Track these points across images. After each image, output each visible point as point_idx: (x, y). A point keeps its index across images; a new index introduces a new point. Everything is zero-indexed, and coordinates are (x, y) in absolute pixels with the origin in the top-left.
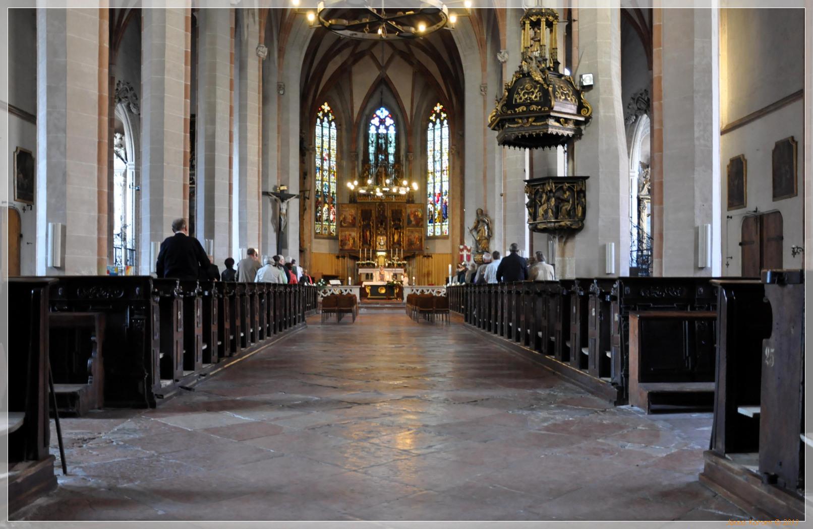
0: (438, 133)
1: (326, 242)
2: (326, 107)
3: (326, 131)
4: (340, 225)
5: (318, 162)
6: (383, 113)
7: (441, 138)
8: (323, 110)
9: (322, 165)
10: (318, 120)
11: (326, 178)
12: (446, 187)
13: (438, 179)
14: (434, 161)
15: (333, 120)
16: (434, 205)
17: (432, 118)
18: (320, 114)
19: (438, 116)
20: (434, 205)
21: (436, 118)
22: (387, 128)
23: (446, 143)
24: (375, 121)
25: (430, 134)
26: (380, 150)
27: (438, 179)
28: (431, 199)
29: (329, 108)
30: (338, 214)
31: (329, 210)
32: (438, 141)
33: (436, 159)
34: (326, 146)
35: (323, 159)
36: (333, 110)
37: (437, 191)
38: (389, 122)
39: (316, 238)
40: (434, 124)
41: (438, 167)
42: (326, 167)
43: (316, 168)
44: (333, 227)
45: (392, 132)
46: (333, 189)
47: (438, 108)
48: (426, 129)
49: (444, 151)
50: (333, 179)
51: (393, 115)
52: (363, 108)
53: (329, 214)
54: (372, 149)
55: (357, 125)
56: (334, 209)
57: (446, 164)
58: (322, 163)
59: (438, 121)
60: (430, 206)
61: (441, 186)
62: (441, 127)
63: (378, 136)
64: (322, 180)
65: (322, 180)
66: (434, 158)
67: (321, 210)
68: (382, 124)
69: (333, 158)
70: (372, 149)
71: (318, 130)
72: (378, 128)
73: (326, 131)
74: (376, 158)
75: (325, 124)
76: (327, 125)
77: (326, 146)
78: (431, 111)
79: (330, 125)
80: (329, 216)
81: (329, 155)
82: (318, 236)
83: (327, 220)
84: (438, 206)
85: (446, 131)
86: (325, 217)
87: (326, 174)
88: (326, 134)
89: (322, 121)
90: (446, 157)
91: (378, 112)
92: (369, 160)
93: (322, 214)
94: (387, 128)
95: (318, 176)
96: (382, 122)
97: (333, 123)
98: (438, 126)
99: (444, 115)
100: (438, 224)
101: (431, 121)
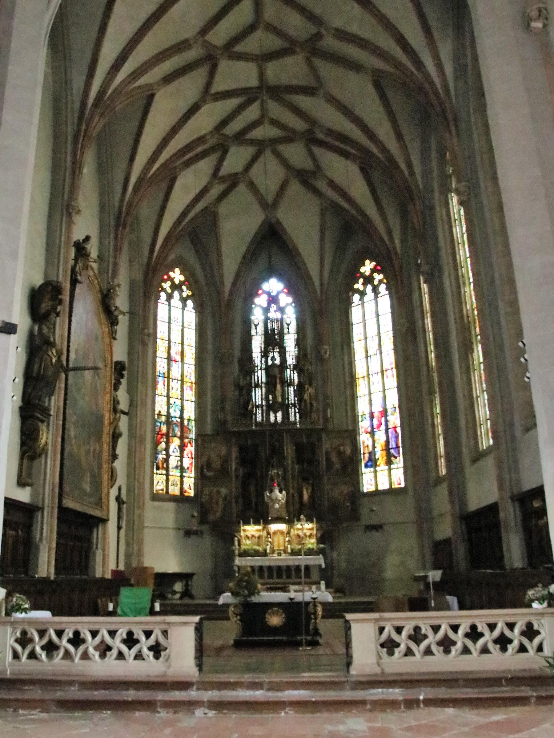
1: (171, 506)
3: (176, 313)
4: (201, 478)
5: (161, 365)
6: (273, 285)
8: (172, 280)
10: (163, 295)
11: (175, 392)
12: (393, 399)
13: (376, 387)
15: (188, 297)
16: (372, 433)
18: (167, 285)
19: (369, 280)
20: (372, 433)
22: (282, 310)
24: (261, 301)
26: (273, 340)
27: (376, 387)
28: (364, 425)
29: (182, 278)
31: (182, 447)
34: (176, 338)
35: (169, 358)
36: (191, 280)
37: (377, 408)
38: (285, 300)
41: (375, 366)
42: (176, 372)
44: (189, 482)
45: (291, 316)
46: (190, 412)
48: (348, 303)
50: (190, 395)
51: (291, 289)
52: (238, 276)
53: (182, 457)
54: (257, 344)
55: (229, 305)
56: (190, 449)
59: (369, 288)
60: (364, 439)
62: (376, 297)
63: (266, 321)
67: (167, 449)
68: (274, 304)
70: (257, 344)
71: (162, 310)
72: (266, 310)
73: (176, 313)
74: (265, 354)
75: (176, 301)
76: (180, 304)
77: (176, 338)
79: (184, 305)
80: (181, 460)
82: (156, 497)
83: (177, 467)
84: (380, 436)
85: (385, 301)
86: (173, 461)
87: (175, 385)
88: (176, 321)
89: (170, 297)
93: (168, 455)
94: (282, 310)
95: (161, 389)
96: (273, 300)
97: (190, 303)
99: (378, 277)
100: (382, 467)
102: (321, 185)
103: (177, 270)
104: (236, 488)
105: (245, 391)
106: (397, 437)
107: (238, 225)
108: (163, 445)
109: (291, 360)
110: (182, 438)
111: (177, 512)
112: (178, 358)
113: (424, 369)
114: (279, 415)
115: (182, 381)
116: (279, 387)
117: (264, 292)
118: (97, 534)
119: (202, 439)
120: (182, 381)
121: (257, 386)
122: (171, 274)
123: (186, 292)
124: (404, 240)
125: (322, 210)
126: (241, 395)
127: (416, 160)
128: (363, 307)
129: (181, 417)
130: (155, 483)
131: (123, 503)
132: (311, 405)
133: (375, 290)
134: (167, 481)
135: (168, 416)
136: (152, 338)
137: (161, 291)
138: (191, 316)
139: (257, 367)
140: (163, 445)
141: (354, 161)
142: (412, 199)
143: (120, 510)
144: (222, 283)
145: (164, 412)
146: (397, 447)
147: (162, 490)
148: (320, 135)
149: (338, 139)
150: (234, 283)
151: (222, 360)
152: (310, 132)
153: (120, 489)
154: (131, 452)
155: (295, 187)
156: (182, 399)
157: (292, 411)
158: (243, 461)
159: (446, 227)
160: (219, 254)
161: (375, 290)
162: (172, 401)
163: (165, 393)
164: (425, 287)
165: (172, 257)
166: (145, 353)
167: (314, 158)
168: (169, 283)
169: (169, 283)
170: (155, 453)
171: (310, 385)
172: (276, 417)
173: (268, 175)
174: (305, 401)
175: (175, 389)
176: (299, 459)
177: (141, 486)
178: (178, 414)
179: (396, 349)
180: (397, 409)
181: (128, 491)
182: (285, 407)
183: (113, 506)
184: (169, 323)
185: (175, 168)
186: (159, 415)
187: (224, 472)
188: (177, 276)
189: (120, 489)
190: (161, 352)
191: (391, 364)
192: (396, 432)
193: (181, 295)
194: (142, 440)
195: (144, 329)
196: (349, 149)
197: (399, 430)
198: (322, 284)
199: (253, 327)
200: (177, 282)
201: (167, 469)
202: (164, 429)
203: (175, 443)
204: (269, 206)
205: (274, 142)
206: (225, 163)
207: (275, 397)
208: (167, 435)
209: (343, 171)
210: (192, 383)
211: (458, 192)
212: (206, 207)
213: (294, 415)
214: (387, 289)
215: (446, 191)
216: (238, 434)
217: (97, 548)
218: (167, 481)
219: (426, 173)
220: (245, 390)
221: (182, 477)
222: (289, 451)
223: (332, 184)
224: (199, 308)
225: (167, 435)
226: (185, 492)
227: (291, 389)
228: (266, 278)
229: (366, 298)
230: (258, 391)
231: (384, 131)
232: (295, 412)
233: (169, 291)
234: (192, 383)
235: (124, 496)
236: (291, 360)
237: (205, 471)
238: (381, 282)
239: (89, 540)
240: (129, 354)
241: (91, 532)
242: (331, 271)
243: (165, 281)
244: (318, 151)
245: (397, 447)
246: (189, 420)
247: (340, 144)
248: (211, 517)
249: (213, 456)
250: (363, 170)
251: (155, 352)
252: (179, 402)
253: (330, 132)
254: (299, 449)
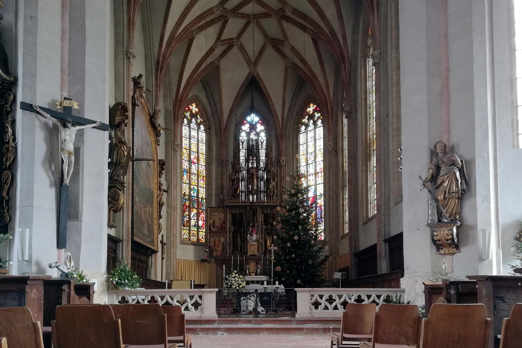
0: (311, 134)
1: (192, 247)
3: (194, 133)
4: (209, 232)
5: (185, 165)
7: (315, 140)
8: (191, 111)
9: (190, 168)
10: (185, 121)
11: (194, 182)
14: (307, 164)
15: (201, 123)
17: (305, 120)
18: (188, 114)
19: (311, 117)
21: (309, 119)
23: (320, 143)
25: (302, 138)
26: (252, 151)
29: (197, 110)
30: (206, 221)
31: (198, 214)
32: (311, 144)
33: (310, 162)
35: (190, 161)
36: (202, 111)
39: (183, 242)
40: (307, 126)
41: (311, 170)
43: (182, 171)
44: (202, 234)
46: (203, 193)
47: (311, 109)
48: (298, 132)
49: (318, 152)
50: (202, 183)
53: (198, 220)
54: (243, 154)
55: (226, 129)
56: (203, 215)
57: (320, 166)
58: (190, 166)
61: (316, 189)
64: (190, 184)
65: (190, 184)
66: (307, 161)
67: (189, 215)
68: (253, 129)
69: (202, 162)
70: (243, 154)
71: (185, 130)
73: (194, 133)
74: (247, 161)
75: (193, 125)
77: (194, 149)
78: (302, 113)
79: (199, 128)
80: (198, 222)
81: (198, 159)
83: (195, 226)
85: (320, 131)
86: (193, 222)
88: (194, 138)
89: (190, 122)
90: (320, 158)
91: (249, 119)
92: (239, 163)
93: (190, 219)
97: (202, 127)
98: (311, 127)
99: (317, 115)
101: (304, 124)
102: (287, 50)
104: (230, 238)
105: (235, 182)
106: (321, 212)
107: (233, 76)
108: (187, 213)
109: (262, 165)
110: (198, 209)
111: (195, 250)
112: (195, 161)
113: (341, 172)
114: (255, 197)
115: (198, 175)
116: (255, 180)
117: (248, 122)
118: (152, 259)
119: (209, 209)
120: (198, 175)
121: (242, 180)
124: (335, 91)
125: (286, 67)
126: (233, 184)
127: (349, 33)
128: (307, 134)
129: (198, 196)
130: (183, 234)
131: (165, 244)
132: (274, 192)
133: (315, 123)
134: (190, 233)
135: (190, 195)
136: (179, 147)
137: (184, 118)
138: (203, 135)
139: (243, 168)
140: (187, 213)
141: (309, 34)
142: (344, 62)
143: (163, 248)
144: (222, 114)
145: (187, 193)
146: (321, 218)
147: (186, 238)
148: (288, 13)
149: (299, 17)
150: (230, 115)
151: (222, 163)
152: (282, 10)
153: (162, 236)
154: (169, 215)
155: (270, 51)
156: (198, 186)
157: (262, 195)
158: (233, 223)
159: (363, 81)
160: (220, 96)
161: (315, 123)
162: (192, 187)
163: (188, 182)
164: (345, 121)
165: (191, 95)
166: (175, 157)
167: (283, 31)
170: (183, 217)
171: (274, 180)
172: (253, 198)
173: (253, 40)
174: (270, 189)
175: (193, 180)
176: (266, 222)
177: (175, 235)
178: (195, 195)
179: (324, 161)
180: (323, 196)
181: (167, 238)
182: (258, 192)
183: (160, 245)
184: (190, 139)
185: (192, 31)
186: (185, 195)
187: (223, 228)
188: (194, 108)
189: (162, 236)
190: (185, 157)
191: (321, 169)
192: (321, 209)
193: (196, 121)
194: (175, 209)
195: (174, 141)
196: (306, 24)
197: (323, 208)
198: (283, 118)
199: (241, 143)
200: (194, 112)
201: (190, 227)
202: (187, 203)
203: (194, 211)
204: (253, 63)
205: (258, 16)
206: (225, 31)
207: (253, 186)
208: (189, 207)
209: (301, 40)
210: (203, 177)
211: (373, 57)
212: (213, 62)
213: (263, 197)
214: (322, 123)
215: (365, 57)
216: (231, 207)
217: (151, 267)
218: (190, 233)
219: (355, 44)
220: (235, 182)
221: (198, 231)
222: (260, 218)
223: (293, 49)
224: (208, 131)
225: (189, 207)
226: (200, 240)
227: (262, 183)
228: (249, 114)
229: (309, 129)
230: (243, 183)
231: (330, 12)
232: (264, 196)
234: (203, 177)
235: (165, 241)
236: (262, 165)
237: (212, 228)
238: (319, 118)
239: (147, 263)
240: (166, 157)
241: (148, 258)
242: (290, 108)
244: (287, 25)
245: (321, 218)
246: (202, 199)
247: (301, 21)
248: (215, 254)
249: (216, 219)
250: (315, 41)
251: (181, 156)
252: (196, 188)
253: (295, 11)
254: (266, 216)
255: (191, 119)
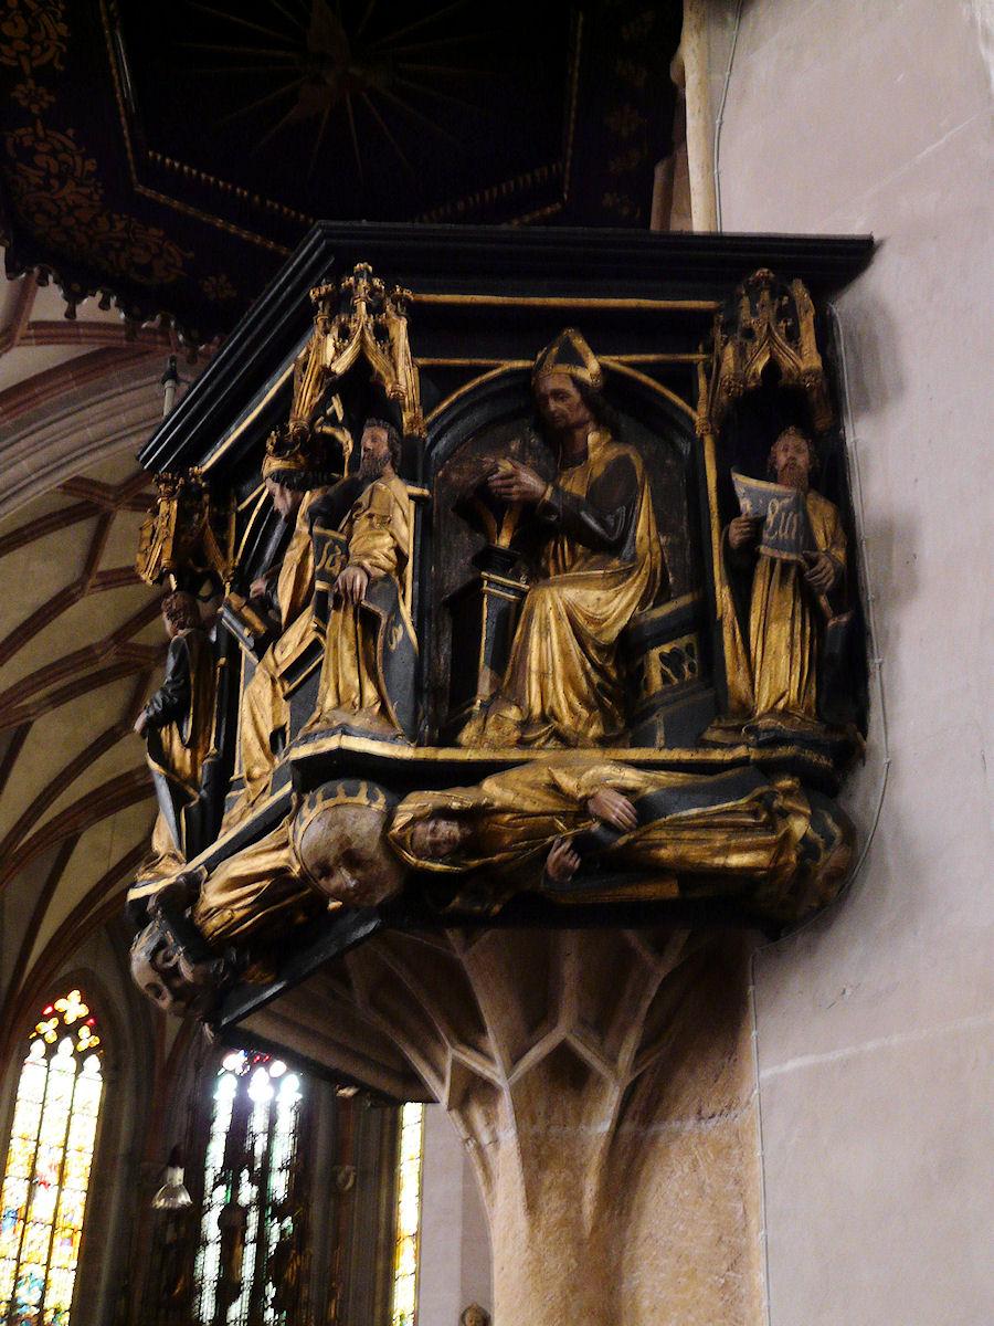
2: (72, 1006)
8: (60, 1015)
10: (38, 1048)
29: (83, 1011)
34: (53, 1135)
36: (100, 1017)
42: (43, 1207)
50: (67, 1256)
76: (73, 1064)
77: (53, 1135)
89: (51, 1050)
97: (93, 1063)
103: (75, 995)
112: (53, 1178)
122: (60, 1005)
123: (87, 1038)
129: (40, 1305)
162: (25, 1270)
168: (54, 1022)
169: (54, 1022)
178: (35, 1298)
188: (72, 1006)
233: (51, 1037)
243: (47, 1018)
252: (40, 1272)
255: (57, 1043)
